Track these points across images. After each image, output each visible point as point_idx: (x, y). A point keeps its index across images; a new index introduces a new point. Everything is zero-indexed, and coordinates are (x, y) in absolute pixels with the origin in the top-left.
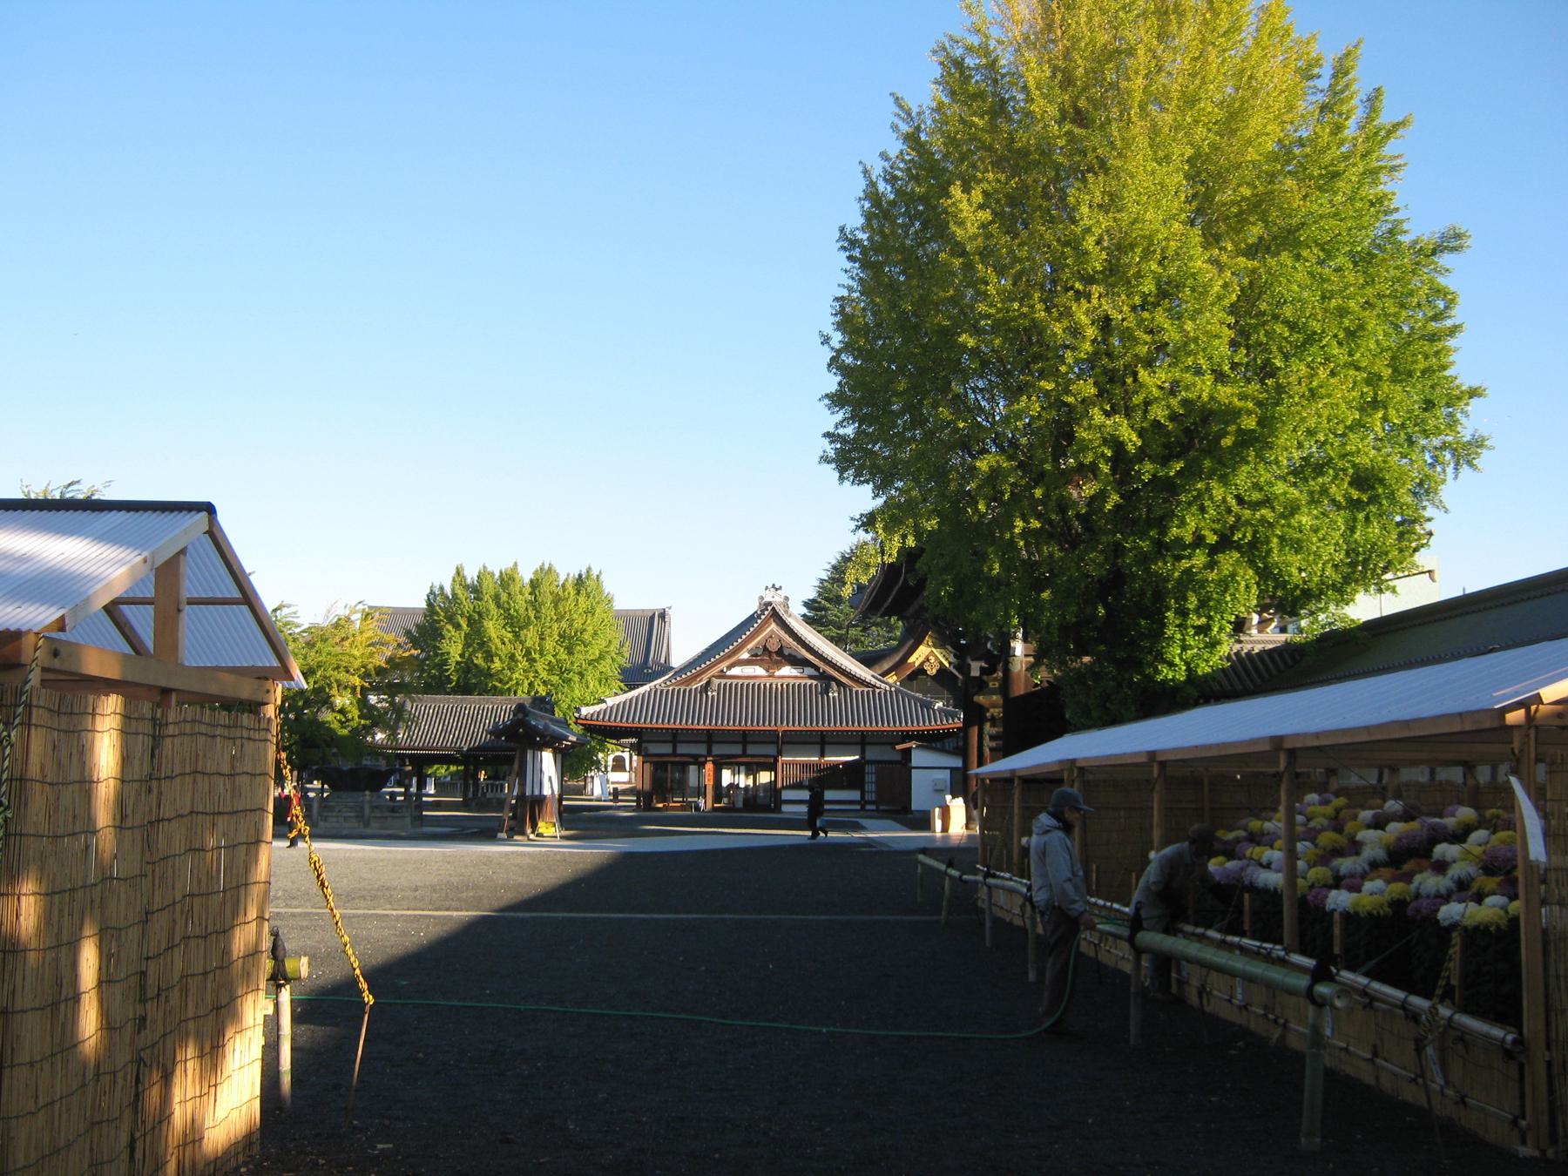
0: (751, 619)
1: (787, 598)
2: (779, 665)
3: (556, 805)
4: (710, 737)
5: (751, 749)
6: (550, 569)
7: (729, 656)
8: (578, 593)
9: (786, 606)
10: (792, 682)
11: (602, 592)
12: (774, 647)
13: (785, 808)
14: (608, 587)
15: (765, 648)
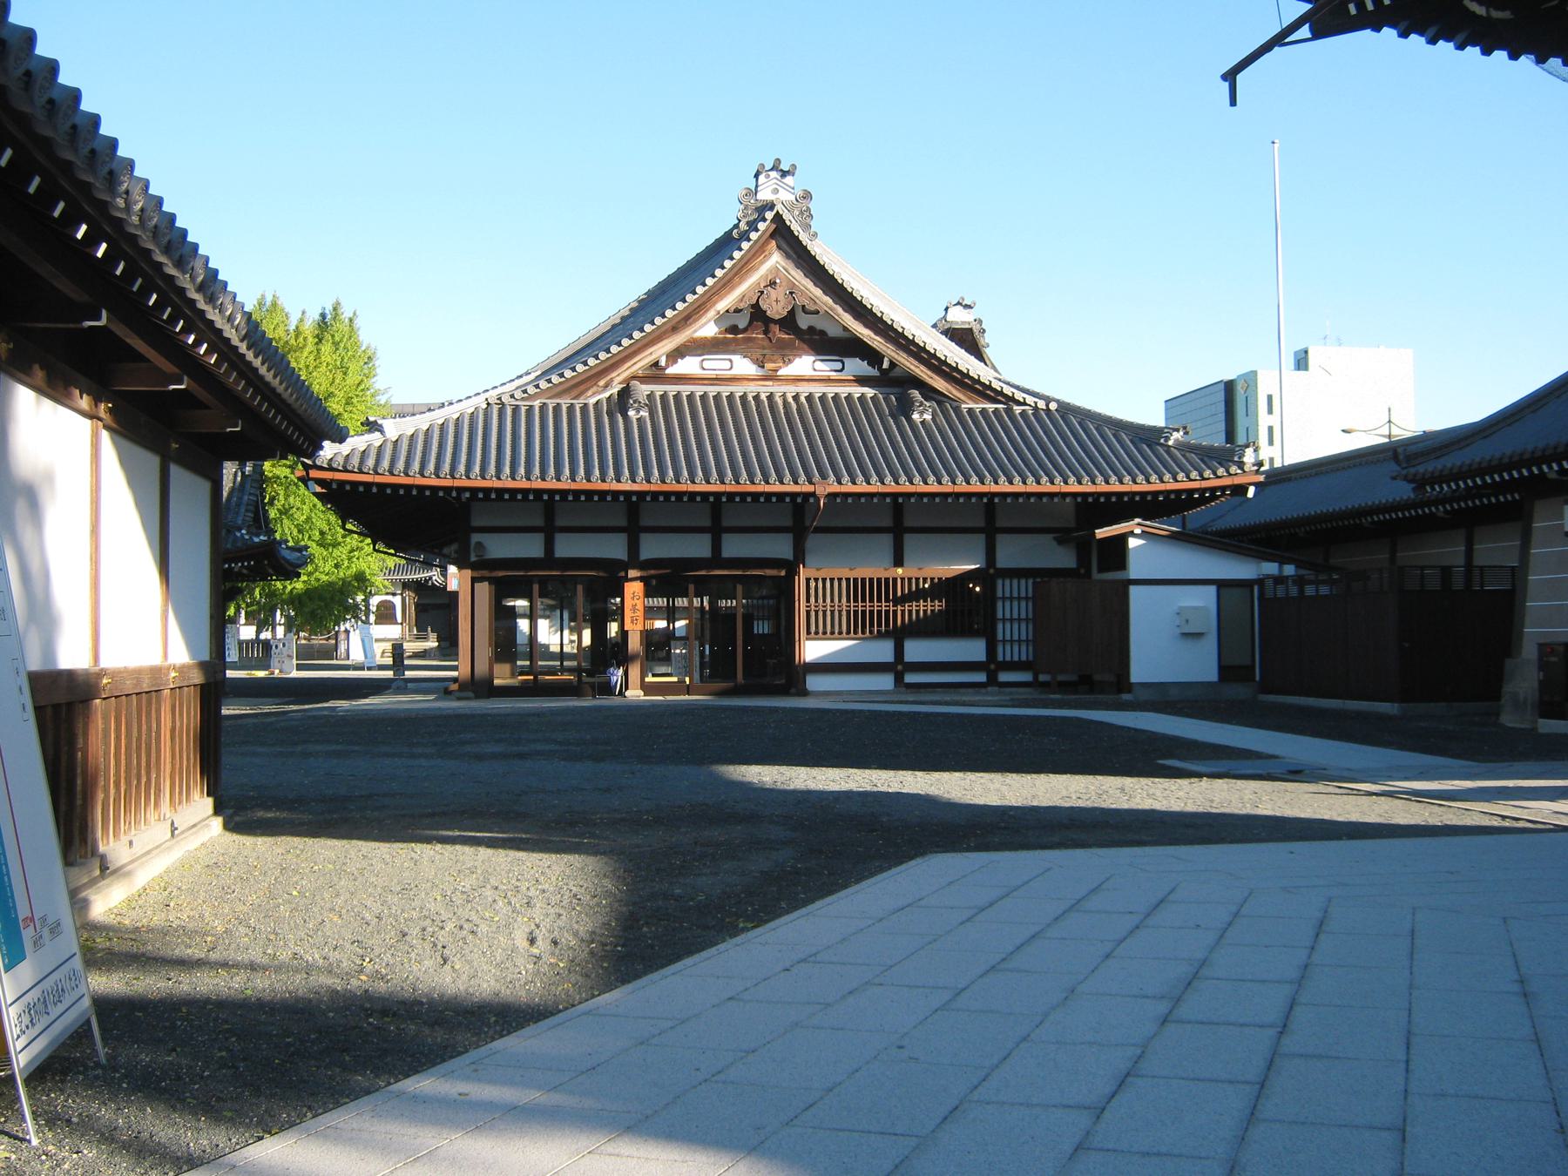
0: (726, 244)
1: (807, 196)
2: (785, 352)
3: (191, 716)
4: (634, 513)
5: (734, 547)
6: (274, 304)
7: (675, 328)
8: (320, 340)
9: (807, 214)
10: (818, 390)
11: (357, 344)
12: (776, 307)
13: (814, 682)
14: (367, 335)
15: (758, 314)
